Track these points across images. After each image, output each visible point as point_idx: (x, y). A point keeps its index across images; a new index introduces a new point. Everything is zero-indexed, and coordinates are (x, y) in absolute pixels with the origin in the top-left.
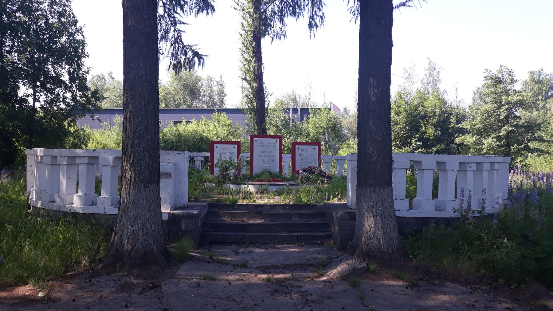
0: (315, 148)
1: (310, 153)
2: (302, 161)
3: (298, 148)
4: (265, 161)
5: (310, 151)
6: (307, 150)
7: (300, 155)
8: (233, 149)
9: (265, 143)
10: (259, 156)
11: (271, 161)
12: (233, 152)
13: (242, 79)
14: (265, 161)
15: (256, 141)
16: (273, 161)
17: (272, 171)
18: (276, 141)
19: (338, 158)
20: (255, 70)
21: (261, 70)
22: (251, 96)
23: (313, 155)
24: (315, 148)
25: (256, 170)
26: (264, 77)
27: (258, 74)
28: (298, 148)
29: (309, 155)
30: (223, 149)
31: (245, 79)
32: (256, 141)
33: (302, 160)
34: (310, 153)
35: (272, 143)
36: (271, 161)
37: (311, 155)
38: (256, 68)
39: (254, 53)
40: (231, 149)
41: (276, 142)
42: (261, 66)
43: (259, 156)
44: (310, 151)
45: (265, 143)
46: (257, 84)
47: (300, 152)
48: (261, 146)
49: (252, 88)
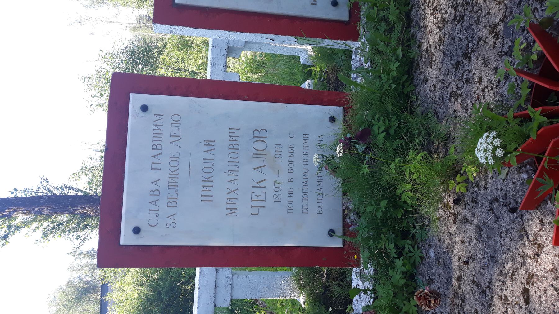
4: (257, 176)
9: (155, 175)
10: (231, 212)
11: (260, 146)
14: (257, 176)
15: (137, 230)
18: (144, 108)
22: (46, 224)
26: (5, 197)
32: (137, 230)
35: (157, 135)
36: (260, 146)
41: (152, 110)
43: (231, 212)
45: (155, 175)
46: (15, 211)
48: (173, 202)
49: (26, 224)
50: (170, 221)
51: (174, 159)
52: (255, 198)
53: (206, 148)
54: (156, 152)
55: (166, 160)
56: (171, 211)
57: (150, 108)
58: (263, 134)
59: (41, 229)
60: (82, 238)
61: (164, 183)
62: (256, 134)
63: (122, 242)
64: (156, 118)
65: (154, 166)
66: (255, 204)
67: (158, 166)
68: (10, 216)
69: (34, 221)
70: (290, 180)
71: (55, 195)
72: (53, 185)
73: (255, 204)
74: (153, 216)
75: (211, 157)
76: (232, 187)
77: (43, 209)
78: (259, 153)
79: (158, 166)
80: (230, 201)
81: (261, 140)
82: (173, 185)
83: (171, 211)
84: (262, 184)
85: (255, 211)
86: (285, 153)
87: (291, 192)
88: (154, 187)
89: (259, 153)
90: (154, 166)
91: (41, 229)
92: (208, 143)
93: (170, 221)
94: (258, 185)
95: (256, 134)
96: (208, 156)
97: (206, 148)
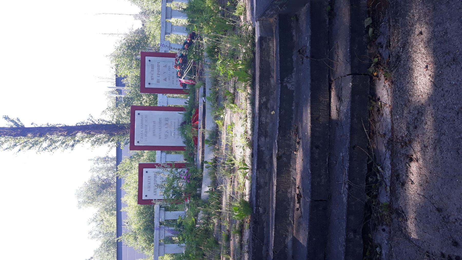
0: (150, 61)
1: (156, 68)
2: (167, 79)
4: (166, 129)
5: (153, 68)
7: (158, 81)
8: (149, 173)
13: (72, 150)
14: (166, 129)
16: (167, 119)
17: (181, 121)
19: (164, 32)
20: (61, 135)
21: (61, 127)
22: (92, 139)
24: (150, 61)
25: (180, 142)
26: (70, 125)
27: (66, 131)
28: (149, 84)
29: (158, 69)
30: (149, 187)
31: (73, 146)
32: (138, 142)
33: (165, 80)
34: (156, 68)
35: (142, 120)
37: (159, 66)
38: (60, 134)
39: (40, 136)
40: (149, 177)
41: (141, 114)
42: (57, 128)
43: (160, 138)
44: (153, 68)
46: (77, 132)
47: (155, 81)
48: (146, 135)
49: (83, 138)
50: (146, 140)
51: (146, 126)
53: (154, 123)
55: (144, 126)
56: (146, 138)
58: (167, 119)
59: (90, 141)
60: (111, 146)
61: (144, 132)
66: (165, 136)
68: (75, 135)
69: (87, 137)
70: (174, 130)
71: (96, 124)
72: (95, 119)
73: (165, 136)
74: (142, 139)
76: (160, 132)
77: (91, 132)
80: (160, 136)
81: (167, 121)
82: (146, 132)
83: (146, 138)
86: (173, 124)
88: (142, 132)
89: (167, 124)
91: (90, 141)
92: (154, 122)
93: (146, 140)
94: (167, 132)
96: (154, 125)
97: (154, 123)
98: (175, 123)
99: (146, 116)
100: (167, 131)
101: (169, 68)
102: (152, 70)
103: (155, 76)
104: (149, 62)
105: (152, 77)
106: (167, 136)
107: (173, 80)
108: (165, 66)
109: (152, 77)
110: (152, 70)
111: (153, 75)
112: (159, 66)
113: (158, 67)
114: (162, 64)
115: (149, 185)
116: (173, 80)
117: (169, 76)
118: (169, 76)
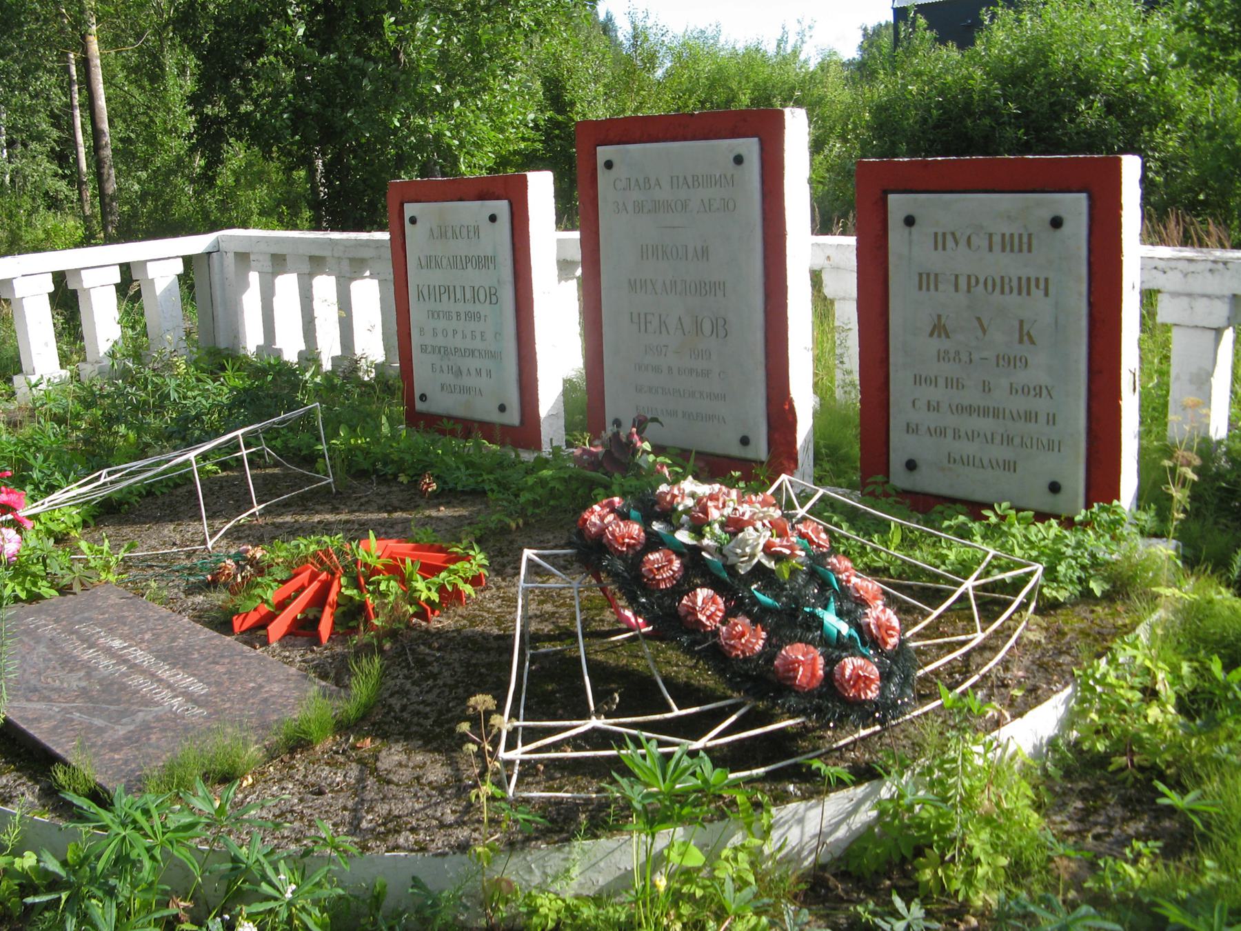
0: (1057, 223)
1: (1010, 265)
2: (944, 344)
3: (910, 221)
6: (980, 241)
7: (927, 280)
10: (632, 285)
11: (707, 327)
12: (490, 254)
16: (721, 327)
23: (1038, 293)
28: (910, 221)
29: (1001, 285)
32: (609, 165)
33: (939, 329)
34: (1010, 265)
36: (707, 327)
37: (1025, 286)
40: (477, 230)
44: (1010, 244)
48: (639, 208)
51: (685, 206)
52: (649, 318)
54: (690, 180)
57: (740, 167)
58: (722, 333)
62: (721, 322)
63: (599, 149)
64: (729, 177)
65: (675, 180)
66: (642, 317)
67: (675, 185)
73: (642, 317)
75: (690, 256)
78: (698, 327)
79: (675, 185)
83: (630, 208)
84: (663, 329)
85: (635, 319)
87: (657, 369)
88: (653, 182)
89: (698, 327)
90: (675, 180)
92: (704, 253)
94: (662, 324)
95: (721, 322)
97: (699, 249)
98: (706, 373)
99: (731, 205)
100: (663, 329)
101: (1010, 362)
102: (997, 239)
103: (960, 261)
104: (1048, 215)
105: (949, 238)
106: (643, 328)
107: (941, 382)
108: (1025, 335)
109: (949, 238)
110: (997, 239)
111: (963, 242)
112: (1025, 286)
113: (1015, 284)
114: (1038, 308)
115: (449, 234)
116: (941, 382)
117: (964, 357)
118: (964, 357)
